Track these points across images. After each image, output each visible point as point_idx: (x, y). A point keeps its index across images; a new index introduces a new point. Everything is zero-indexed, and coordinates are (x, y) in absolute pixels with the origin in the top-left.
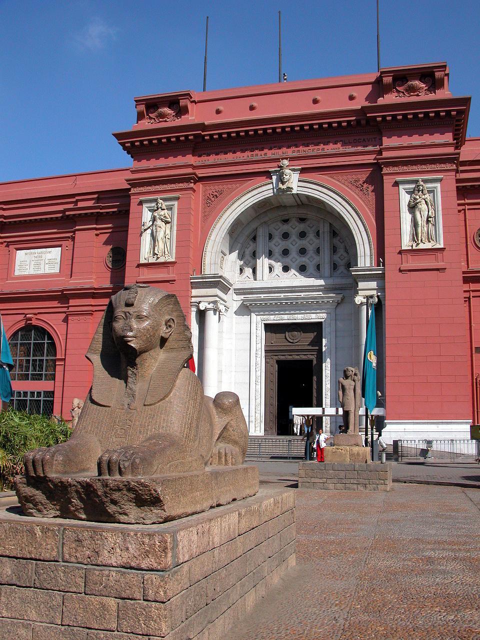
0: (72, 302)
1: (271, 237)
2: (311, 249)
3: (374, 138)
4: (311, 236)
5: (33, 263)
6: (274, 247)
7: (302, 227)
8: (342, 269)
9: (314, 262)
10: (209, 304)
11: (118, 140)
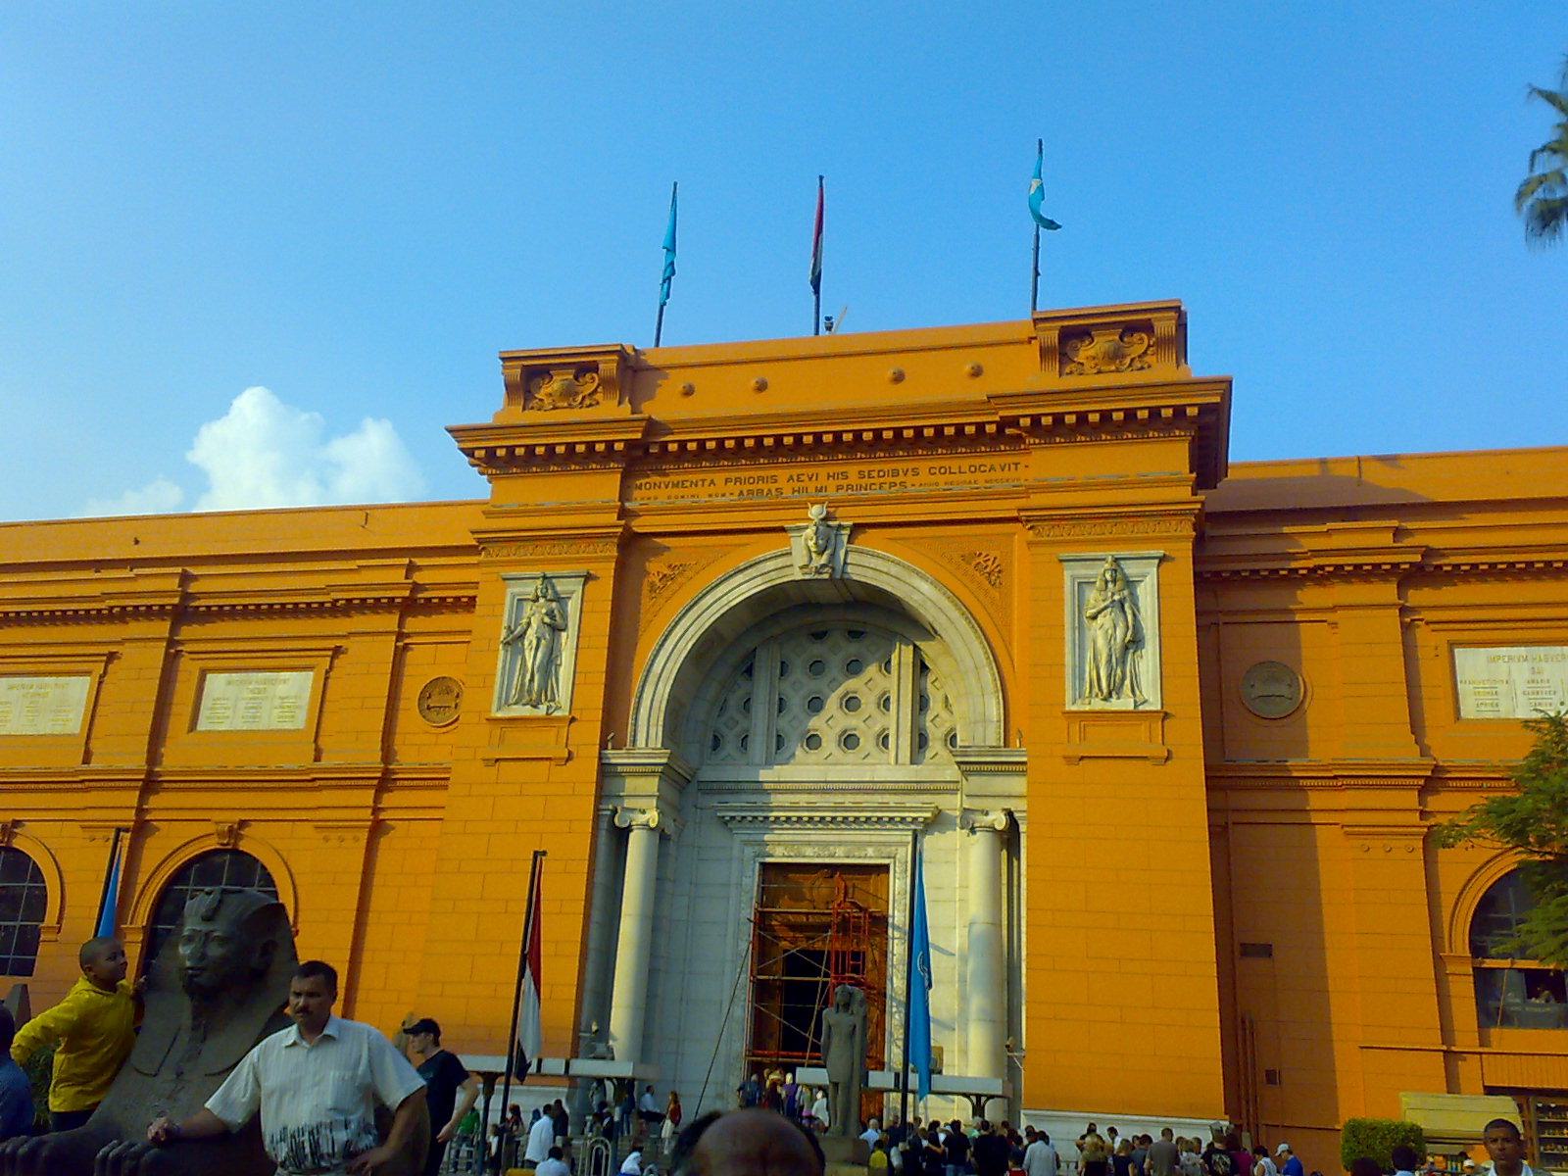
2: (869, 702)
3: (1016, 464)
4: (872, 670)
5: (242, 705)
7: (852, 649)
8: (936, 746)
9: (877, 728)
11: (458, 442)
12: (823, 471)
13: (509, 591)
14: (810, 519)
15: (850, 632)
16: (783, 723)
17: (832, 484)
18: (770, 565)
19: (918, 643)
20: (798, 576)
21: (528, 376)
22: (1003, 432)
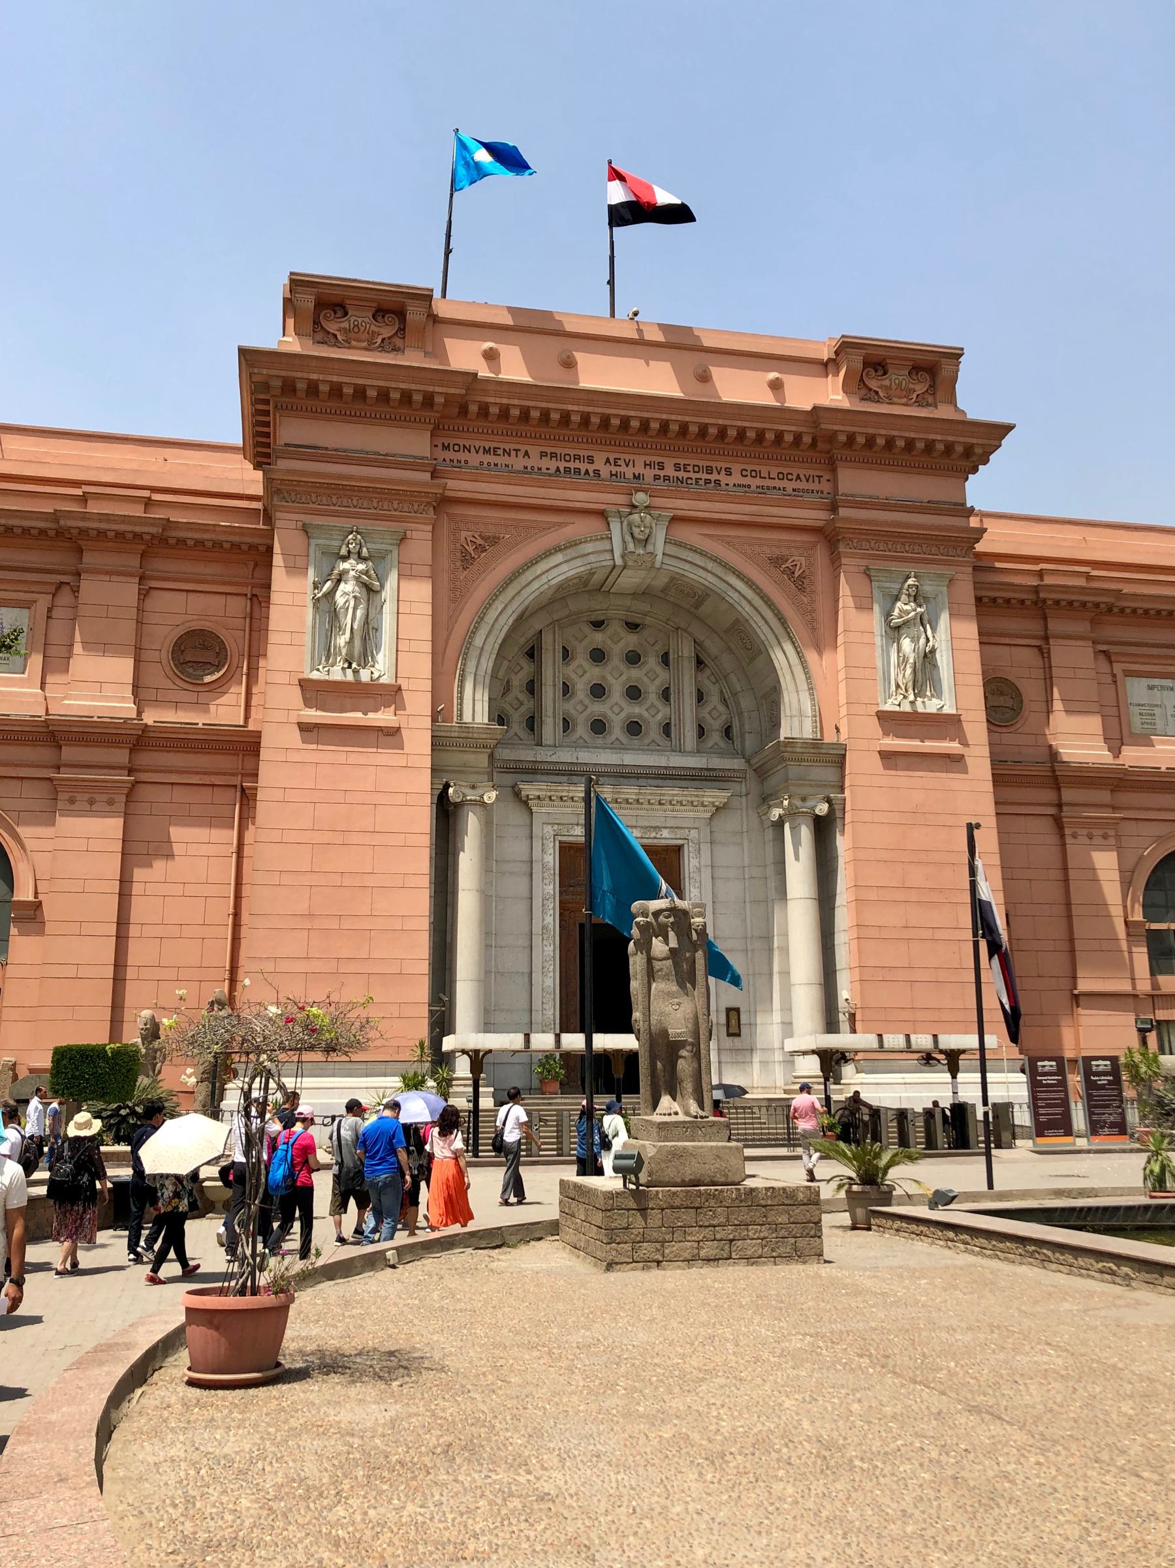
0: (69, 753)
1: (566, 653)
2: (652, 690)
3: (820, 477)
6: (574, 676)
7: (631, 641)
9: (659, 716)
10: (473, 787)
12: (640, 460)
13: (313, 542)
14: (636, 507)
15: (627, 624)
16: (570, 707)
17: (649, 473)
18: (589, 547)
19: (701, 638)
20: (619, 561)
21: (318, 303)
22: (815, 443)
